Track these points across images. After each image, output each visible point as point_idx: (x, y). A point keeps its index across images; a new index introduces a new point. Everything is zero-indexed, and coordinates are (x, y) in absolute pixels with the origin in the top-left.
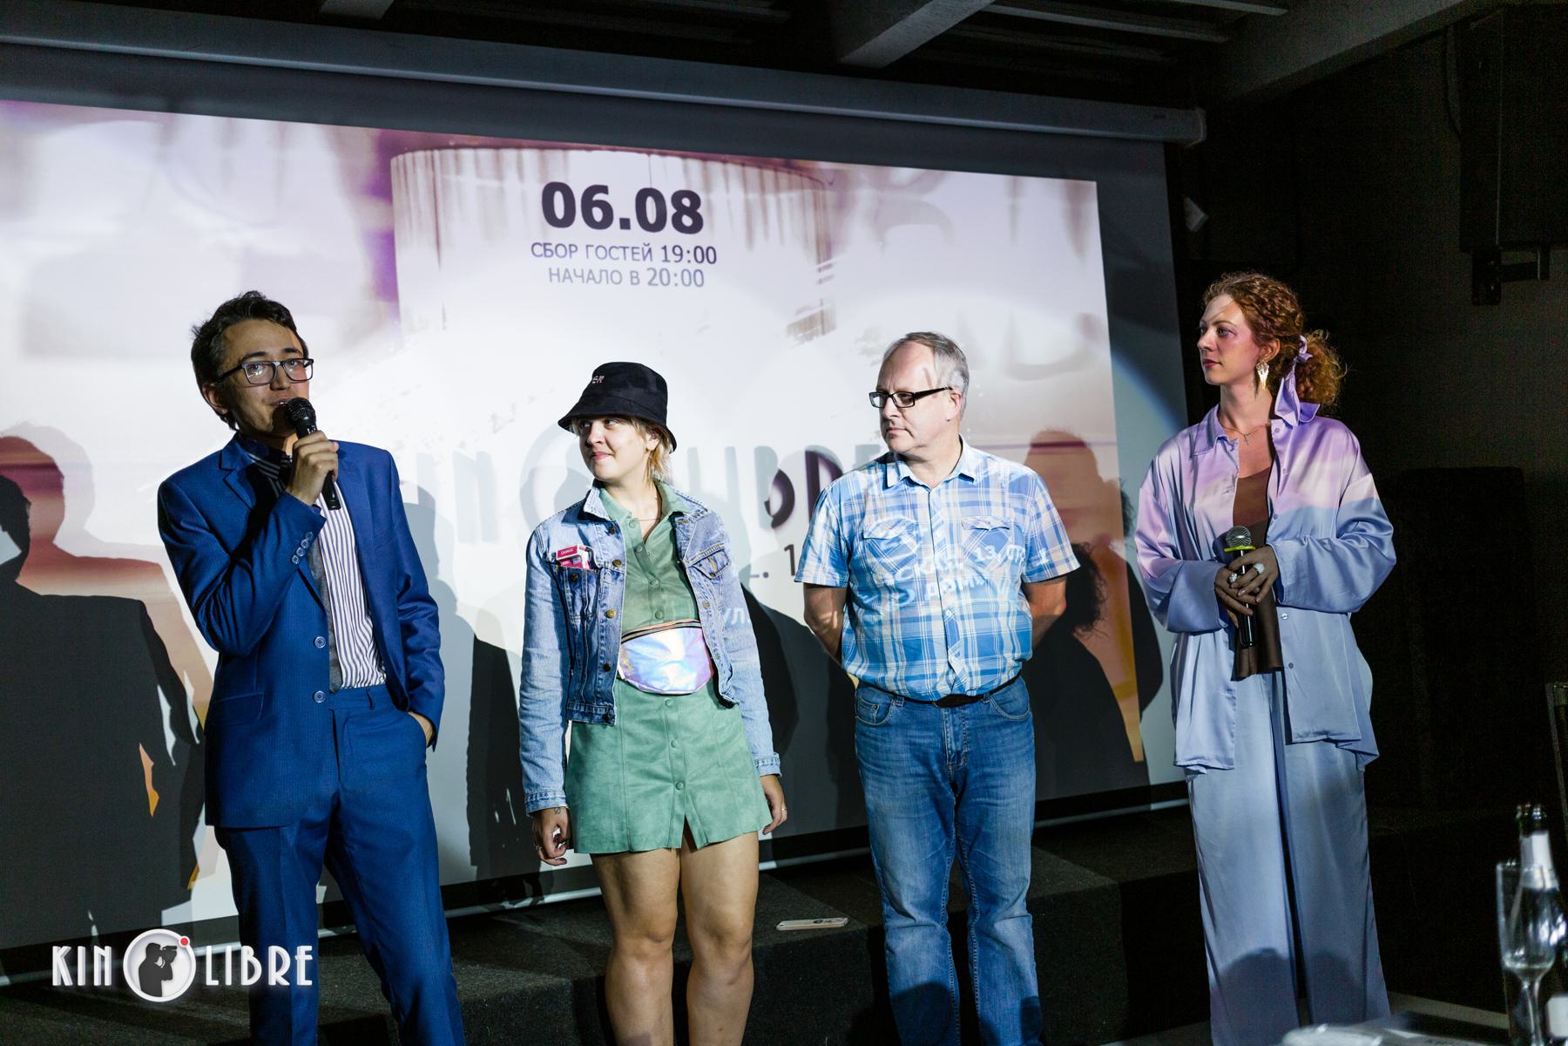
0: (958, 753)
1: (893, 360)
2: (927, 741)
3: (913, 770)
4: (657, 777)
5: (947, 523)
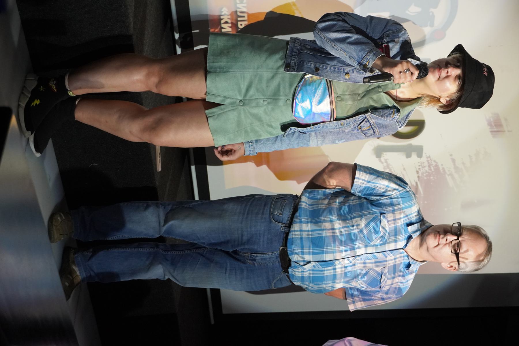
0: (255, 260)
1: (477, 232)
2: (261, 243)
3: (245, 233)
4: (247, 90)
5: (386, 259)
